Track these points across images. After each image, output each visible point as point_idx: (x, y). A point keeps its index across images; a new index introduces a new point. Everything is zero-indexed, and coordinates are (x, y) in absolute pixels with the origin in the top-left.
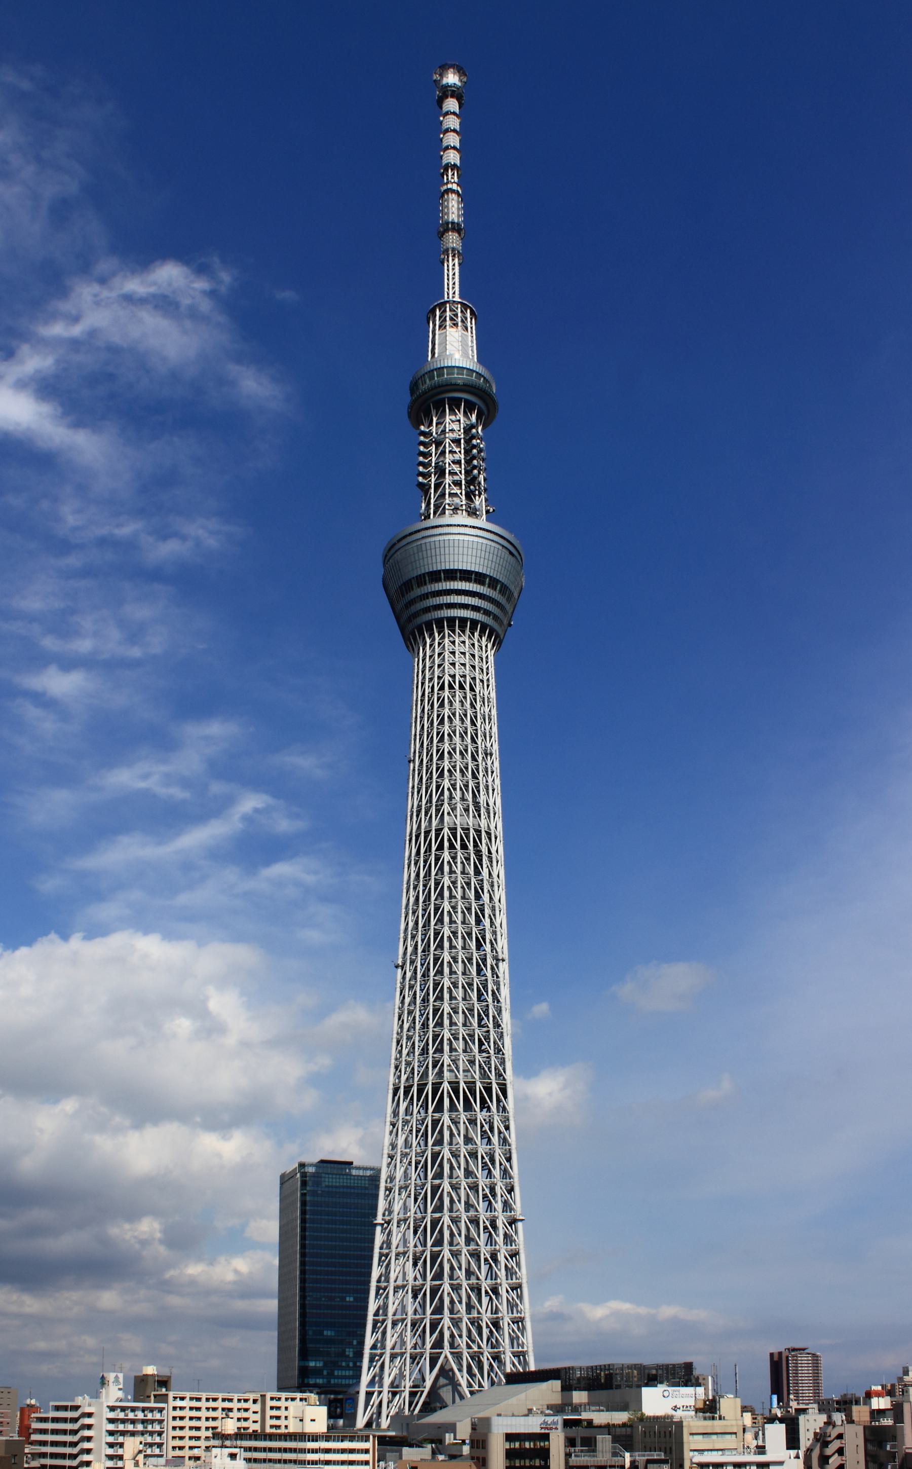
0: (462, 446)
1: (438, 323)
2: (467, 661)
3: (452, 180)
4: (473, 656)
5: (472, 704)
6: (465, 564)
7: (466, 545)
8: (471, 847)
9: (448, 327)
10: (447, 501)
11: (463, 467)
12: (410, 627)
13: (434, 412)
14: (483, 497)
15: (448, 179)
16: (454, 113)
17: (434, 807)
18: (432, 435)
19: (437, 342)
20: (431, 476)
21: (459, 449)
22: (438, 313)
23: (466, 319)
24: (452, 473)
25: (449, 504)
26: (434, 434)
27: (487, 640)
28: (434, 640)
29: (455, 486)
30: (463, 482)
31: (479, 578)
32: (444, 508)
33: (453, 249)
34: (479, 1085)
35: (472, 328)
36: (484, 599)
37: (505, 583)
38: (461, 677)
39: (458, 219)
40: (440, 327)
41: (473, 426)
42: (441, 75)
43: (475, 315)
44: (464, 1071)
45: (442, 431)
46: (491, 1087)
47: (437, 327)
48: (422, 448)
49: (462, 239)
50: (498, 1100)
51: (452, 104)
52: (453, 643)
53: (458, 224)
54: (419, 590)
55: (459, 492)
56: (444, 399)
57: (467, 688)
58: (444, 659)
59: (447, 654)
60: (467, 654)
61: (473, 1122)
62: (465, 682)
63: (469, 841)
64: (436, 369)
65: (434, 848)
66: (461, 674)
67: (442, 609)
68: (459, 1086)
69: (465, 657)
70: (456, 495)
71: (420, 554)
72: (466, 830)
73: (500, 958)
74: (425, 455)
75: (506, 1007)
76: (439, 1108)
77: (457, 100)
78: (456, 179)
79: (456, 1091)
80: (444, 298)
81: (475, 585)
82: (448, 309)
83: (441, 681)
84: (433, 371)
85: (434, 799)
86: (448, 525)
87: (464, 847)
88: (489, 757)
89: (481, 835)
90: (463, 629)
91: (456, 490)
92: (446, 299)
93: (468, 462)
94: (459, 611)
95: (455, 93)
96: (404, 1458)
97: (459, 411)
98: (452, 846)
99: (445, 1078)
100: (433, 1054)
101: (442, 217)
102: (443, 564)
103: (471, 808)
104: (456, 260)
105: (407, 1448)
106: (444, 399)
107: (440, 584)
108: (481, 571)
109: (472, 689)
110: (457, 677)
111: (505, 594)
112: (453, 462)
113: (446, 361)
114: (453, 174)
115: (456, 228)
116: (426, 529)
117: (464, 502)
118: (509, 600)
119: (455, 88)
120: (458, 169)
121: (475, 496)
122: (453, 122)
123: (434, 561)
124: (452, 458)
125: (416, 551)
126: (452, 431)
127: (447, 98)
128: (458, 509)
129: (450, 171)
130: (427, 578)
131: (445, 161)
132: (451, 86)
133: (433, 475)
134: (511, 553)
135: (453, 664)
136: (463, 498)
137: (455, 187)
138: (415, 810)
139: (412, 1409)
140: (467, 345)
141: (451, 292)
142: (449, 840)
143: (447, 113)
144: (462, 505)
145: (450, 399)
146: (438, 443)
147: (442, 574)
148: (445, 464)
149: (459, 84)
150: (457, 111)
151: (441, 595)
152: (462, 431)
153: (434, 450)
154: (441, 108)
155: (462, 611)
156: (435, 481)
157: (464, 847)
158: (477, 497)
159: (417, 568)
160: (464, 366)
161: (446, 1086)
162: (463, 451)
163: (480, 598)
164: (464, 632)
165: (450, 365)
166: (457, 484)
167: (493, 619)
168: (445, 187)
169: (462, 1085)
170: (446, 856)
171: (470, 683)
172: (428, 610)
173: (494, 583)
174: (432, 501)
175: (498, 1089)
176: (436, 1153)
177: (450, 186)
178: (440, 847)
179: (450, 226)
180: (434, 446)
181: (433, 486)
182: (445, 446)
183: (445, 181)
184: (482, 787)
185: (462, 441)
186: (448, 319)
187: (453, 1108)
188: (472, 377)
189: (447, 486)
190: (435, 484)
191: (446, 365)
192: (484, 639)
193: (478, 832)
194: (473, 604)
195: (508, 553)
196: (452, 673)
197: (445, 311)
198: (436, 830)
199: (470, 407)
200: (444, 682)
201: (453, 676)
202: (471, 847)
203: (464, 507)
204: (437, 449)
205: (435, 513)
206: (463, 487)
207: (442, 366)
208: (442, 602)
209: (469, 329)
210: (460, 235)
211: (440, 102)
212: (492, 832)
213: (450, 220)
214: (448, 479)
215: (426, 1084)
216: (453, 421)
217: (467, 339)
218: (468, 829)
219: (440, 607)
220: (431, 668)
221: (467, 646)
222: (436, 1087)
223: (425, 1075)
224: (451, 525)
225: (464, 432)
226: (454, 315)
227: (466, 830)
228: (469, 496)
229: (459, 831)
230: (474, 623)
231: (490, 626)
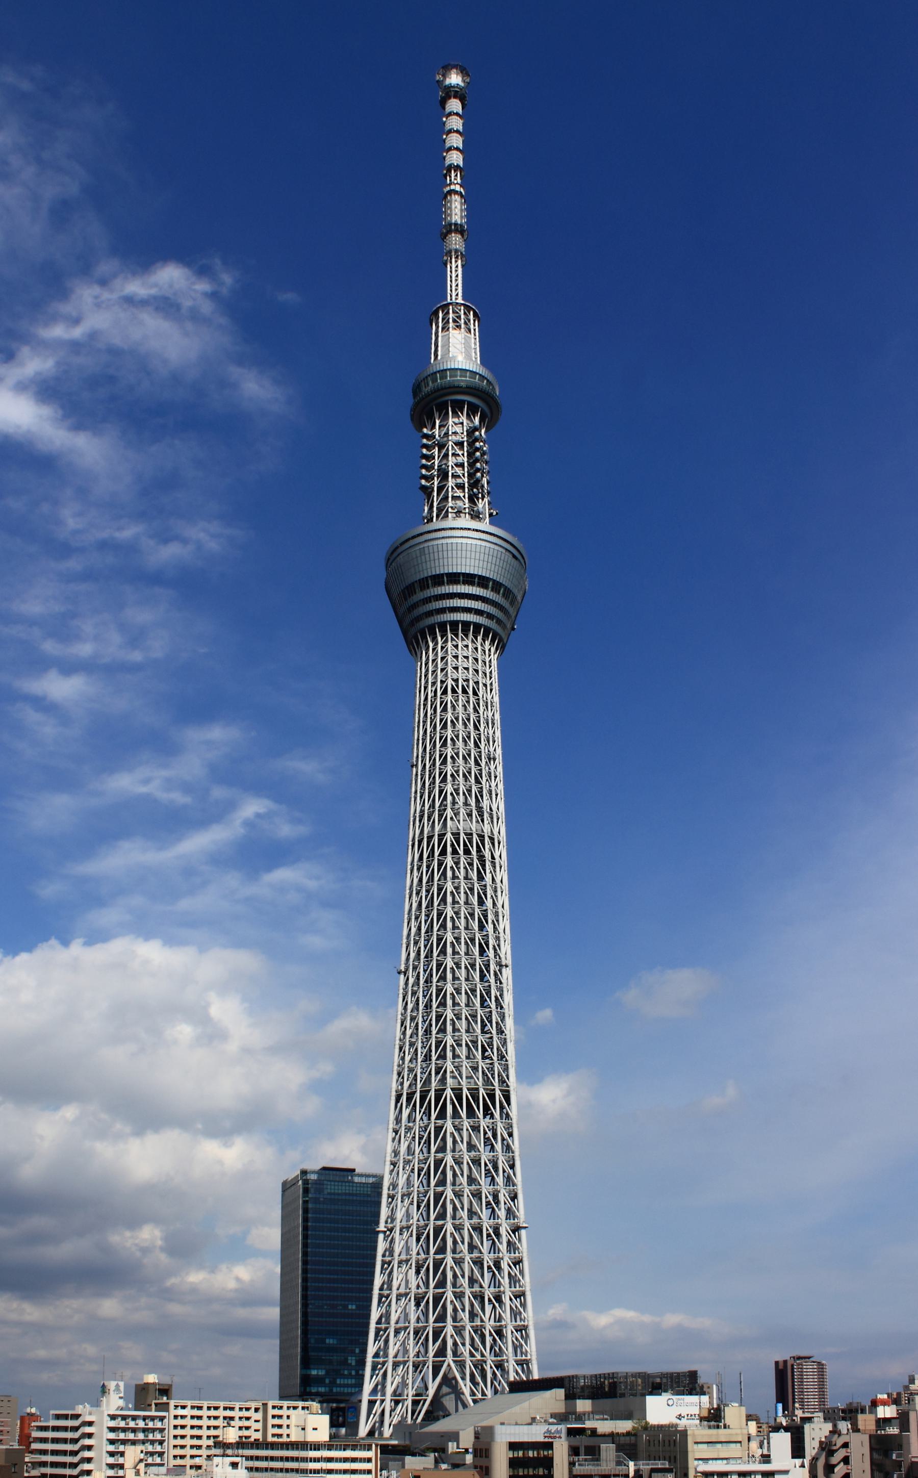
0: (465, 449)
1: (440, 325)
2: (470, 665)
3: (455, 182)
4: (476, 660)
5: (475, 708)
6: (468, 568)
7: (469, 548)
8: (474, 852)
9: (451, 329)
10: (450, 504)
11: (466, 469)
12: (413, 631)
13: (436, 415)
14: (486, 500)
15: (450, 180)
16: (457, 114)
17: (437, 812)
18: (434, 437)
19: (440, 344)
20: (433, 479)
21: (462, 452)
22: (441, 315)
23: (469, 321)
24: (455, 476)
25: (452, 507)
26: (437, 436)
27: (490, 644)
28: (437, 644)
29: (458, 489)
30: (466, 485)
31: (482, 581)
32: (447, 511)
33: (456, 251)
34: (482, 1092)
35: (475, 330)
36: (487, 603)
37: (509, 587)
38: (464, 681)
39: (461, 220)
40: (443, 329)
41: (476, 429)
42: (444, 76)
43: (478, 317)
44: (467, 1078)
45: (445, 434)
46: (495, 1094)
47: (440, 329)
48: (424, 451)
49: (465, 240)
50: (502, 1107)
51: (455, 105)
52: (456, 647)
53: (461, 225)
54: (422, 593)
55: (462, 495)
56: (447, 401)
57: (471, 692)
58: (446, 663)
59: (450, 658)
60: (470, 658)
61: (476, 1128)
62: (468, 686)
63: (472, 847)
64: (439, 372)
65: (437, 853)
66: (464, 678)
67: (445, 612)
68: (462, 1093)
69: (468, 661)
70: (459, 498)
71: (423, 557)
72: (469, 835)
73: (504, 964)
74: (428, 457)
75: (510, 1013)
76: (442, 1115)
77: (460, 101)
78: (459, 180)
79: (459, 1097)
80: (447, 300)
81: (478, 589)
82: (451, 311)
83: (444, 686)
84: (435, 373)
85: (437, 804)
86: (451, 529)
87: (467, 852)
88: (492, 762)
89: (484, 840)
90: (466, 633)
91: (459, 493)
92: (449, 301)
93: (471, 465)
94: (462, 614)
95: (458, 93)
96: (406, 1467)
97: (462, 414)
98: (454, 852)
99: (448, 1085)
100: (436, 1060)
101: (445, 219)
102: (446, 568)
103: (475, 813)
104: (459, 262)
105: (410, 1457)
106: (447, 401)
107: (443, 588)
108: (484, 575)
109: (475, 693)
110: (460, 681)
111: (509, 598)
112: (456, 465)
113: (449, 363)
114: (456, 175)
115: (459, 229)
116: (429, 532)
117: (467, 506)
118: (512, 603)
119: (458, 88)
120: (461, 170)
121: (478, 499)
122: (456, 123)
123: (437, 564)
124: (455, 461)
125: (418, 555)
126: (455, 433)
127: (450, 98)
128: (461, 512)
129: (453, 172)
130: (430, 582)
131: (447, 162)
132: (454, 87)
133: (436, 478)
134: (514, 556)
135: (456, 668)
136: (466, 501)
137: (458, 188)
138: (417, 815)
139: (414, 1417)
140: (470, 347)
141: (454, 294)
142: (452, 845)
143: (450, 114)
144: (465, 508)
145: (453, 401)
146: (441, 446)
147: (445, 578)
148: (448, 466)
149: (462, 84)
150: (460, 112)
151: (444, 599)
152: (465, 433)
153: (436, 453)
154: (444, 108)
155: (465, 615)
156: (438, 484)
157: (467, 852)
158: (480, 500)
159: (419, 572)
160: (467, 368)
161: (449, 1093)
162: (466, 454)
163: (483, 602)
164: (467, 636)
165: (453, 367)
166: (461, 487)
167: (496, 622)
168: (448, 189)
169: (465, 1092)
170: (449, 861)
171: (473, 688)
172: (430, 613)
173: (497, 586)
174: (435, 504)
175: (501, 1096)
176: (439, 1160)
177: (453, 187)
178: (443, 853)
179: (453, 227)
180: (437, 448)
181: (435, 489)
182: (448, 449)
183: (448, 182)
184: (485, 792)
185: (465, 444)
186: (451, 320)
187: (456, 1115)
188: (475, 379)
189: (450, 489)
190: (438, 487)
191: (449, 367)
192: (487, 643)
193: (481, 837)
194: (476, 607)
195: (511, 556)
196: (455, 677)
197: (448, 313)
198: (439, 835)
199: (473, 410)
200: (447, 686)
201: (456, 681)
202: (474, 852)
203: (467, 510)
204: (439, 452)
205: (438, 516)
206: (466, 490)
207: (445, 368)
208: (444, 606)
209: (472, 331)
210: (463, 236)
211: (443, 103)
212: (496, 837)
213: (453, 221)
214: (451, 482)
215: (429, 1091)
216: (456, 424)
217: (471, 341)
218: (471, 834)
219: (442, 611)
220: (433, 672)
221: (470, 650)
222: (439, 1094)
223: (427, 1082)
224: (454, 529)
225: (467, 435)
226: (457, 317)
227: (469, 835)
228: (472, 499)
229: (462, 836)
230: (477, 627)
231: (493, 630)
